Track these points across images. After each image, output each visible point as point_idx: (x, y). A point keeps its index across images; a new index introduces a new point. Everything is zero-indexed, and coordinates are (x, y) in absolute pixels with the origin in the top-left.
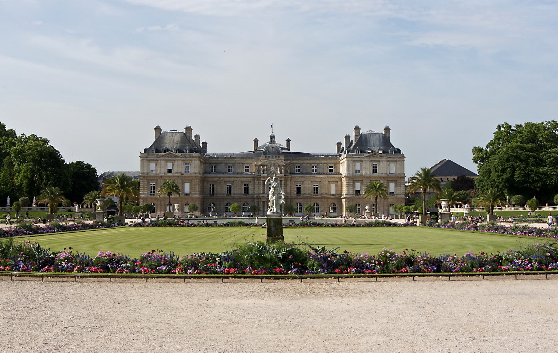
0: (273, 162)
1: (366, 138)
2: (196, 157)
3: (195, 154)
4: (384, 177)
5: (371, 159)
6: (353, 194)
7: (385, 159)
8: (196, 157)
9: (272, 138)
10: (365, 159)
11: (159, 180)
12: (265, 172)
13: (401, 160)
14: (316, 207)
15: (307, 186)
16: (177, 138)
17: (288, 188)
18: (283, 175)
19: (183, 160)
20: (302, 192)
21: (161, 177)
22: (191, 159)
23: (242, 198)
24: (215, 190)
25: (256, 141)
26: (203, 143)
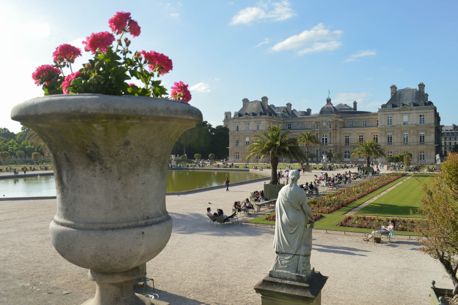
0: (324, 119)
1: (400, 95)
2: (263, 118)
3: (263, 116)
4: (414, 128)
5: (401, 112)
6: (385, 143)
7: (415, 112)
9: (329, 101)
10: (396, 112)
17: (338, 139)
19: (255, 121)
20: (350, 142)
22: (260, 120)
26: (307, 110)
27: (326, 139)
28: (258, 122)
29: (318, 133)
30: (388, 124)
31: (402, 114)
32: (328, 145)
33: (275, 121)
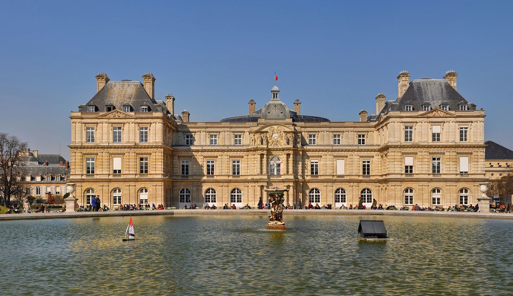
1: (419, 88)
2: (157, 118)
3: (155, 114)
7: (453, 119)
8: (157, 118)
13: (482, 119)
14: (340, 194)
15: (328, 163)
16: (131, 90)
18: (291, 146)
21: (103, 147)
23: (230, 181)
24: (190, 169)
25: (252, 103)
27: (279, 165)
28: (144, 126)
29: (265, 152)
30: (406, 140)
31: (432, 122)
32: (283, 178)
33: (169, 125)
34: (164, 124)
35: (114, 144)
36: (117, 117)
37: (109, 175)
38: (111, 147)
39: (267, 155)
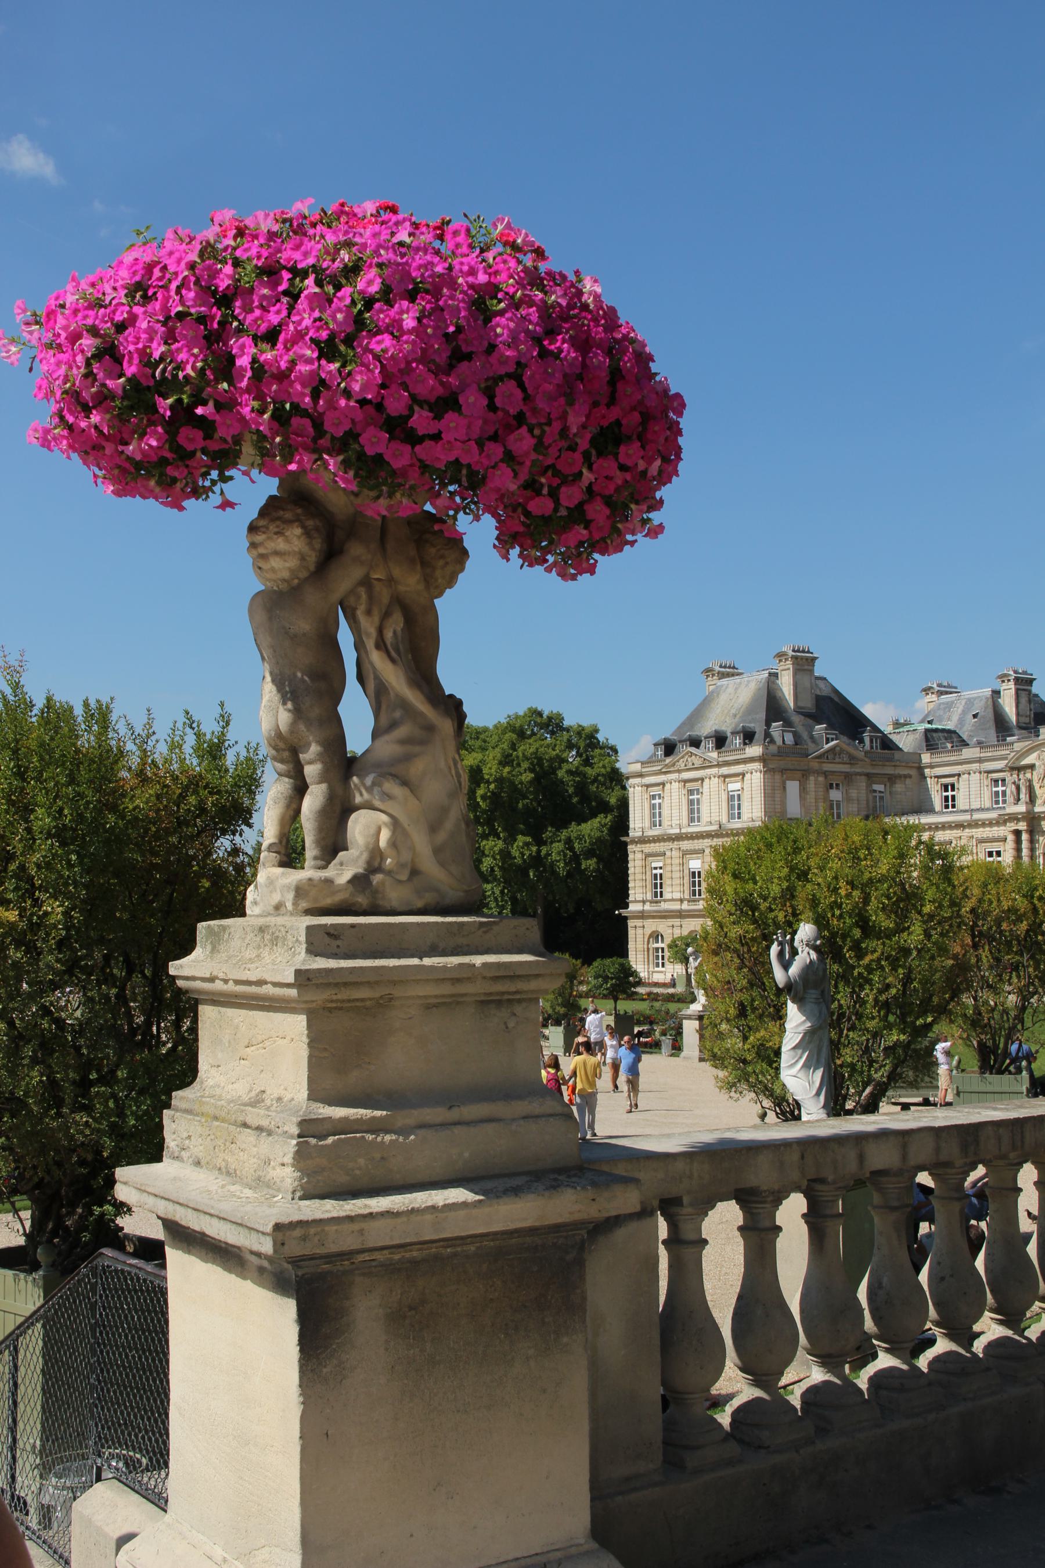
2: (752, 760)
8: (752, 760)
11: (668, 853)
12: (1022, 796)
19: (725, 777)
29: (1022, 826)
34: (768, 771)
35: (691, 830)
36: (690, 766)
37: (681, 901)
38: (679, 837)
39: (1031, 832)
